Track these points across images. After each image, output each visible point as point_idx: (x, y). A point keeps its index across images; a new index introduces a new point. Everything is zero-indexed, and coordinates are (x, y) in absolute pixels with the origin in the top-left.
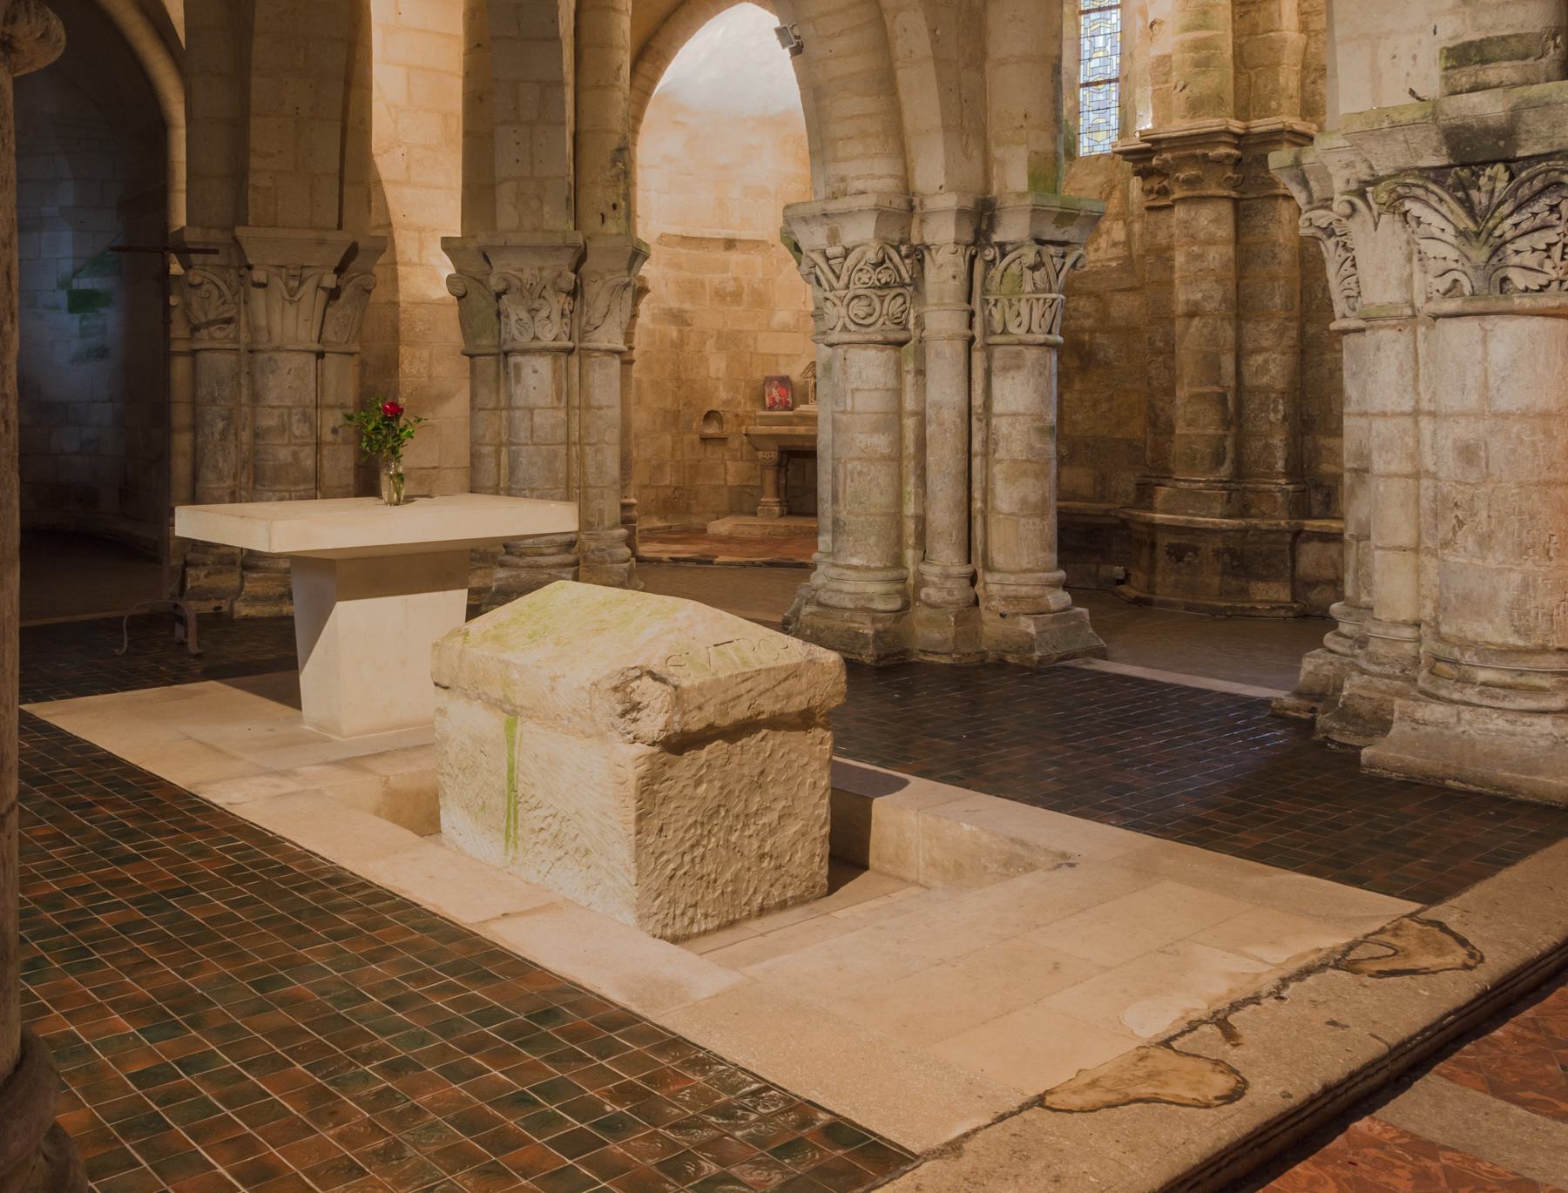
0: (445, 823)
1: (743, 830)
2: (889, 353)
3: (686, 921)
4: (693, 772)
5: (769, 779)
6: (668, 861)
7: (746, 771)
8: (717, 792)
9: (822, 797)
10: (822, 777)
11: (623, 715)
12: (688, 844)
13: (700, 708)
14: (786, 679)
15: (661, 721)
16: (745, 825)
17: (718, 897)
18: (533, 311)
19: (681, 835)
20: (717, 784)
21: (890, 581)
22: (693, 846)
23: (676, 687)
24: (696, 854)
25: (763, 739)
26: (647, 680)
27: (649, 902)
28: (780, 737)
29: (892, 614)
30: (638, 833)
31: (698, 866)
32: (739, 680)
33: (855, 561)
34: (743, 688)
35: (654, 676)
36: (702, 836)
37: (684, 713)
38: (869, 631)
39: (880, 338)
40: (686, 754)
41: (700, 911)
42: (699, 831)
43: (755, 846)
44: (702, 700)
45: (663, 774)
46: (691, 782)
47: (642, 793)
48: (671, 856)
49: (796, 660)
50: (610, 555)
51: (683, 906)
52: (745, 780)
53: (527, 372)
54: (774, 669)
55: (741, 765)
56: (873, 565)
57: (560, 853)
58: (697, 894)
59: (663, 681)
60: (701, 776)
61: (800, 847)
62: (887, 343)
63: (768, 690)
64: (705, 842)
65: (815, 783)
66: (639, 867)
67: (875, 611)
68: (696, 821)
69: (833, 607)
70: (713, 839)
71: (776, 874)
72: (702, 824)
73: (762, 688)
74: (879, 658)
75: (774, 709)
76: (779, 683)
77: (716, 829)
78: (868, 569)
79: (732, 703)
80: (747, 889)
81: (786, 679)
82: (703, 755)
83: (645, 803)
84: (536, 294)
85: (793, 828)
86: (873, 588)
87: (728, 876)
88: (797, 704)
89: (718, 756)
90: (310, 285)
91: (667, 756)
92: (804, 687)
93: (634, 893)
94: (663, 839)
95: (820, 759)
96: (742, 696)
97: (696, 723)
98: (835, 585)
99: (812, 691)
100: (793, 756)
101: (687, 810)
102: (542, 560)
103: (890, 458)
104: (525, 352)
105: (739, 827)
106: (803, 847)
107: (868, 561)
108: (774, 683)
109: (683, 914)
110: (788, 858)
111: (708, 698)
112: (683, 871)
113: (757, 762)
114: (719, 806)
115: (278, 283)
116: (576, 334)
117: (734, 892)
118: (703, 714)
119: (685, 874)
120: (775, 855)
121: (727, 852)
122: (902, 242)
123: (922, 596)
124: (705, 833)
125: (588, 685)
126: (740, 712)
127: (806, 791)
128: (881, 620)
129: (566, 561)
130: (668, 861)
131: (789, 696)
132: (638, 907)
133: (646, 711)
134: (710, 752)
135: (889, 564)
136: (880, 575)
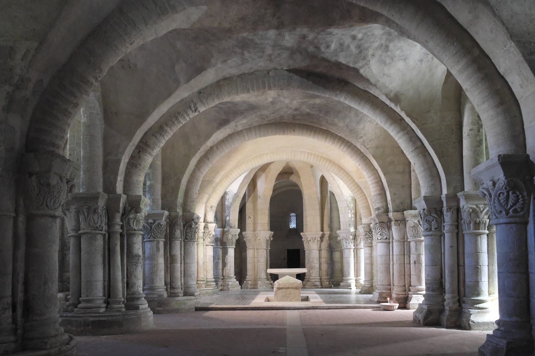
2: (369, 248)
15: (277, 286)
16: (288, 298)
18: (346, 242)
21: (369, 282)
28: (293, 290)
38: (364, 289)
39: (366, 246)
53: (346, 252)
62: (369, 246)
82: (283, 290)
84: (346, 240)
90: (316, 240)
97: (281, 287)
103: (369, 264)
104: (346, 249)
115: (311, 240)
116: (355, 245)
122: (370, 231)
126: (287, 286)
131: (293, 286)
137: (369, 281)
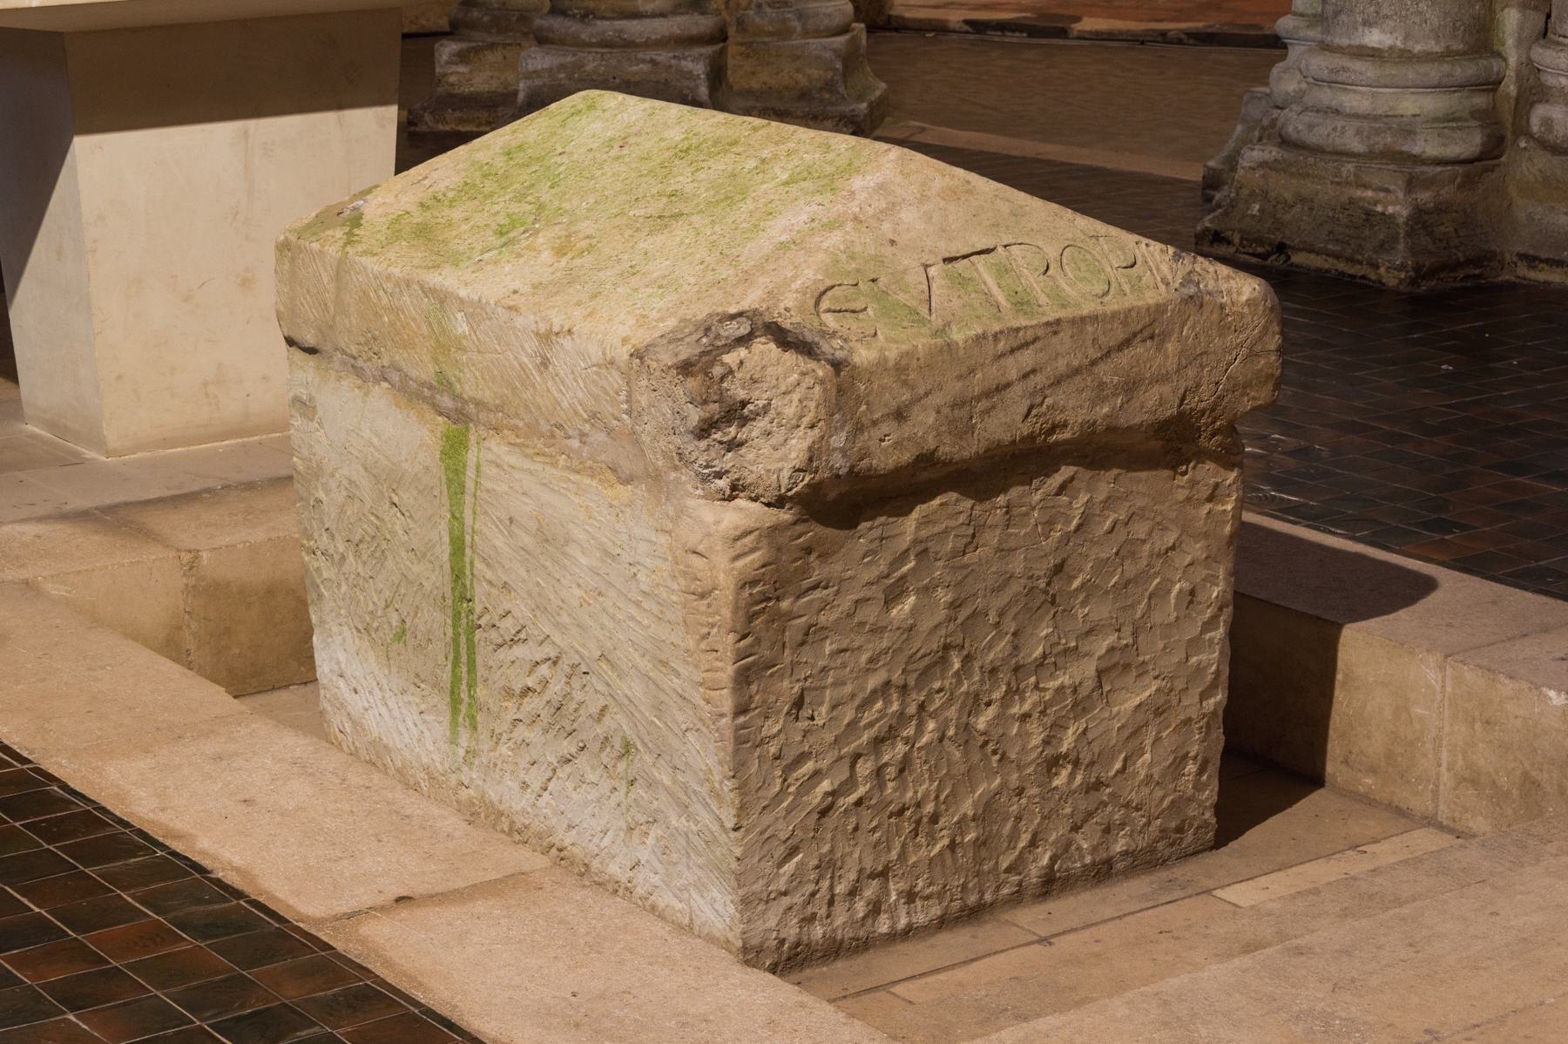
0: (324, 665)
1: (1006, 701)
3: (860, 908)
4: (883, 567)
5: (1076, 584)
6: (817, 775)
7: (1017, 564)
8: (941, 614)
9: (1210, 625)
10: (1212, 579)
11: (703, 431)
12: (866, 737)
13: (900, 415)
14: (1126, 343)
15: (798, 446)
16: (1013, 692)
17: (940, 853)
19: (848, 714)
20: (944, 596)
22: (878, 742)
23: (837, 365)
24: (886, 758)
25: (1061, 489)
26: (765, 348)
27: (768, 866)
28: (1106, 483)
29: (1460, 169)
30: (741, 710)
31: (890, 785)
32: (1002, 346)
33: (1375, 38)
34: (1012, 368)
35: (784, 339)
36: (902, 717)
37: (859, 429)
38: (1398, 209)
40: (864, 525)
41: (895, 888)
42: (895, 707)
43: (1036, 740)
44: (906, 396)
45: (805, 571)
46: (877, 592)
47: (751, 617)
48: (824, 764)
49: (1151, 298)
50: (801, 16)
51: (852, 876)
52: (1015, 587)
54: (1094, 318)
55: (1004, 551)
56: (1418, 48)
57: (568, 747)
58: (889, 849)
59: (806, 348)
60: (903, 578)
61: (1148, 742)
63: (1077, 371)
64: (910, 731)
65: (1192, 593)
66: (742, 788)
67: (1418, 160)
68: (887, 684)
69: (1317, 150)
70: (931, 725)
71: (1084, 805)
72: (904, 689)
73: (1061, 365)
74: (1419, 275)
75: (1090, 417)
76: (1108, 354)
77: (938, 701)
78: (1404, 57)
79: (983, 404)
80: (1014, 836)
81: (1126, 343)
82: (909, 526)
83: (758, 641)
85: (1133, 697)
86: (1410, 105)
87: (967, 807)
88: (1154, 403)
89: (946, 531)
91: (814, 531)
92: (1172, 363)
93: (730, 847)
94: (803, 724)
95: (1206, 535)
96: (1009, 385)
98: (1326, 96)
99: (1191, 373)
100: (1140, 529)
101: (864, 657)
102: (634, 28)
105: (996, 695)
106: (1157, 740)
107: (1406, 38)
108: (1094, 354)
109: (853, 893)
110: (1118, 765)
111: (922, 391)
112: (853, 798)
113: (1048, 544)
114: (947, 647)
117: (980, 844)
118: (907, 430)
119: (859, 803)
120: (1086, 757)
121: (966, 754)
123: (1535, 126)
124: (912, 709)
125: (623, 353)
127: (1170, 609)
128: (1429, 183)
129: (694, 31)
130: (817, 775)
131: (1131, 387)
132: (739, 878)
133: (762, 424)
134: (926, 521)
135: (1458, 46)
136: (1434, 72)
137: (1434, 72)
